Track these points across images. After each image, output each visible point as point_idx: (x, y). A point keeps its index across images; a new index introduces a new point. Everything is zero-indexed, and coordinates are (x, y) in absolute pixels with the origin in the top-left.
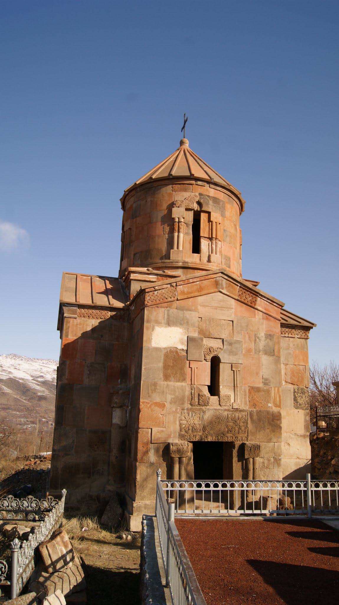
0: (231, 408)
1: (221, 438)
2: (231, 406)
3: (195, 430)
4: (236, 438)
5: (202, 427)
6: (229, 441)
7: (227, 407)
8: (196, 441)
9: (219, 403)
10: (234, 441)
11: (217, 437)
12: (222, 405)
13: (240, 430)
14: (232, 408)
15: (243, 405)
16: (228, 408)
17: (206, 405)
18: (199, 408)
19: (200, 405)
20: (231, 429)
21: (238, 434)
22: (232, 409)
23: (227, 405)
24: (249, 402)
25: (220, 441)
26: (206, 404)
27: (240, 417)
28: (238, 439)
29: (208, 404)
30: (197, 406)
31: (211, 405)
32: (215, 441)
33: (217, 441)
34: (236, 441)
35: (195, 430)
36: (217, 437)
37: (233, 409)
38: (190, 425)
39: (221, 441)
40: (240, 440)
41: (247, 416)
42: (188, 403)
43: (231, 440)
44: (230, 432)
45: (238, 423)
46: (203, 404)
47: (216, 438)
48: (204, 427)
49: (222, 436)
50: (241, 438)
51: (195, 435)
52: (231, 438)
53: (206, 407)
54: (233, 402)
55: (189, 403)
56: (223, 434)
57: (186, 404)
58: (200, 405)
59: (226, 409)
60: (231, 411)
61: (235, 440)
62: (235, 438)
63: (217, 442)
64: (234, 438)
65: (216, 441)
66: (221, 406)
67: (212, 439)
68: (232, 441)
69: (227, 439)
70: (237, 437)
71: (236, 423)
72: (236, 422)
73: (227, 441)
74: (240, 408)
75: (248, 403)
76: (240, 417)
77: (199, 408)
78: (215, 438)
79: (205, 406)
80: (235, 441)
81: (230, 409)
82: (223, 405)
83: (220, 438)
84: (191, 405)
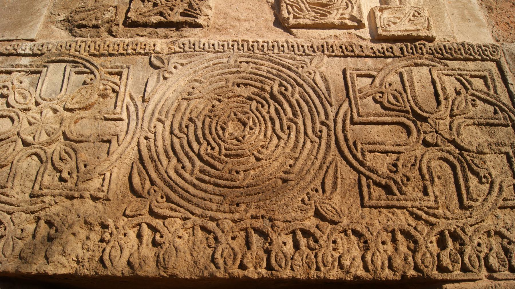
0: (368, 36)
1: (297, 246)
2: (367, 29)
3: (62, 180)
4: (450, 243)
5: (128, 161)
6: (387, 274)
7: (333, 32)
8: (50, 270)
9: (270, 16)
10: (435, 274)
11: (255, 238)
12: (292, 21)
13: (473, 181)
14: (377, 38)
15: (448, 21)
16: (344, 40)
17: (178, 26)
18: (127, 40)
19: (134, 24)
20: (384, 170)
21: (462, 206)
22: (377, 46)
23: (337, 22)
24: (490, 9)
25: (286, 273)
26: (176, 18)
27: (450, 91)
28: (468, 250)
29: (188, 19)
30: (110, 33)
31: (220, 29)
32: (236, 272)
33: (263, 272)
34: (457, 273)
35: (62, 180)
36: (255, 238)
37: (385, 45)
38: (26, 144)
39: (300, 274)
40: (493, 261)
41: (499, 84)
42: (50, 21)
43: (398, 262)
44: (377, 192)
45: (443, 126)
46: (154, 19)
47: (248, 244)
48: (141, 159)
49: (306, 233)
50: (495, 242)
51: (50, 223)
52: (403, 248)
53: (181, 36)
54: (376, 3)
55: (62, 17)
56: (318, 214)
57: (39, 26)
58: (134, 24)
59: (331, 41)
60: (369, 52)
61: (446, 261)
62: (442, 244)
63: (262, 280)
64: (434, 248)
65: (251, 273)
66: (288, 29)
67: (213, 260)
68: (411, 273)
69: (357, 253)
70: (455, 236)
71: (425, 127)
72: (425, 120)
73: (361, 272)
74: (433, 33)
75: (481, 14)
76: (450, 91)
77: (127, 40)
78: (238, 244)
79: (173, 33)
80: (442, 269)
81: (363, 43)
82: (301, 21)
83: (289, 248)
84: (71, 31)
